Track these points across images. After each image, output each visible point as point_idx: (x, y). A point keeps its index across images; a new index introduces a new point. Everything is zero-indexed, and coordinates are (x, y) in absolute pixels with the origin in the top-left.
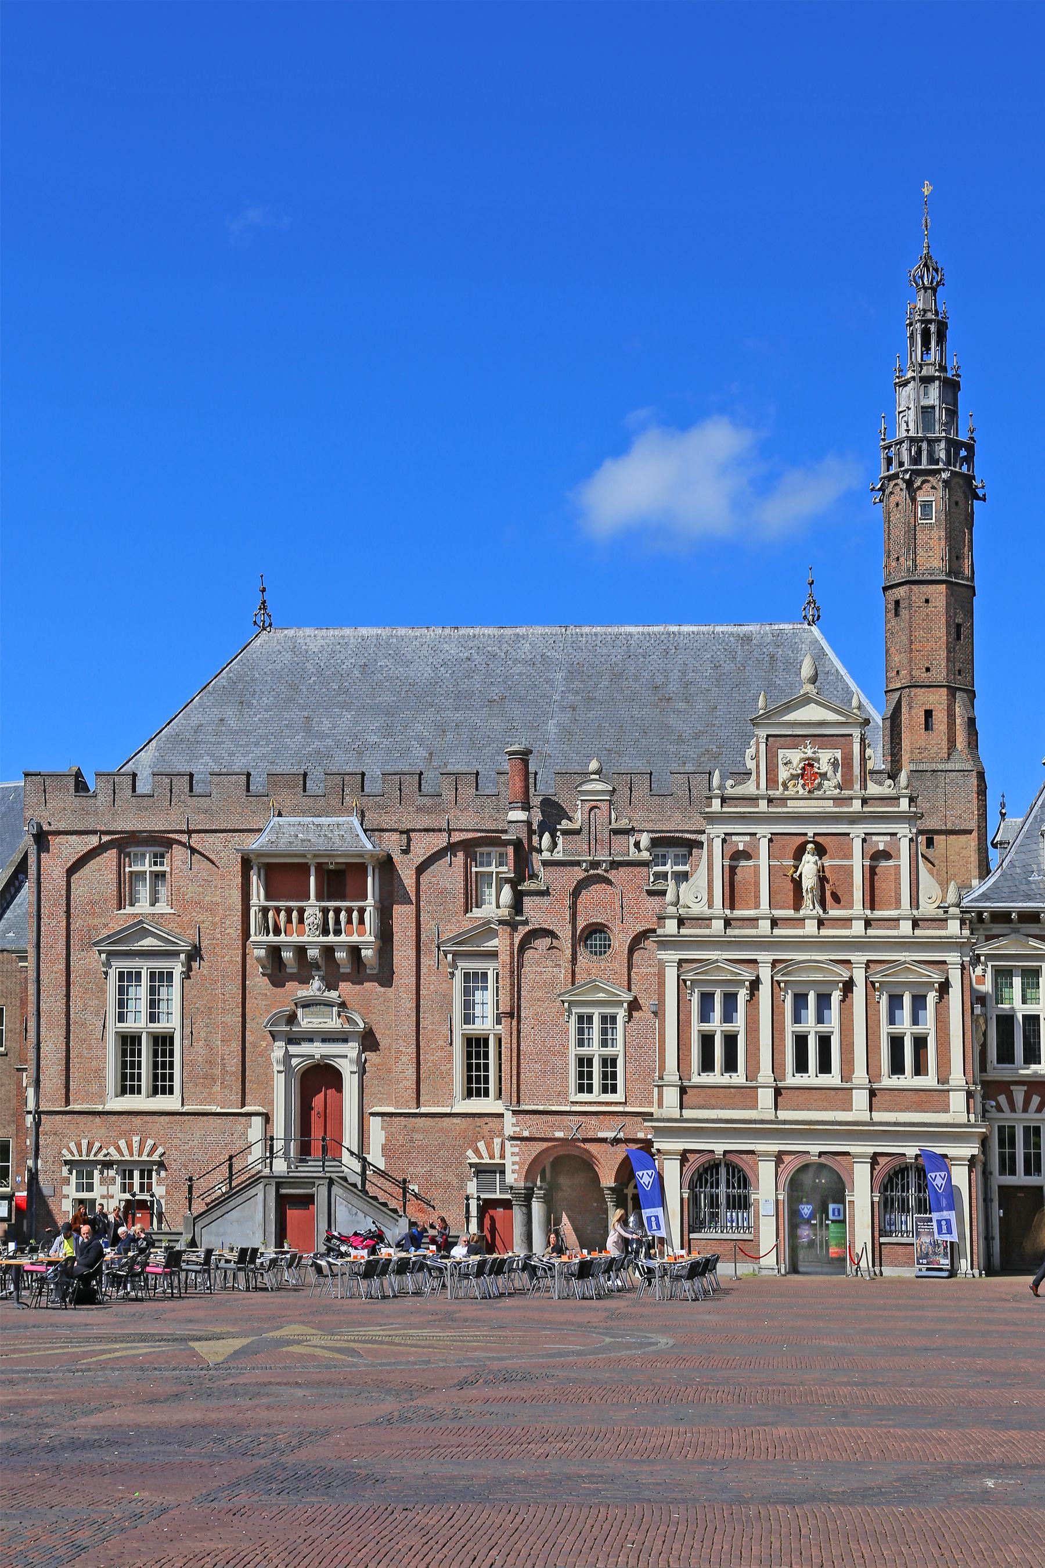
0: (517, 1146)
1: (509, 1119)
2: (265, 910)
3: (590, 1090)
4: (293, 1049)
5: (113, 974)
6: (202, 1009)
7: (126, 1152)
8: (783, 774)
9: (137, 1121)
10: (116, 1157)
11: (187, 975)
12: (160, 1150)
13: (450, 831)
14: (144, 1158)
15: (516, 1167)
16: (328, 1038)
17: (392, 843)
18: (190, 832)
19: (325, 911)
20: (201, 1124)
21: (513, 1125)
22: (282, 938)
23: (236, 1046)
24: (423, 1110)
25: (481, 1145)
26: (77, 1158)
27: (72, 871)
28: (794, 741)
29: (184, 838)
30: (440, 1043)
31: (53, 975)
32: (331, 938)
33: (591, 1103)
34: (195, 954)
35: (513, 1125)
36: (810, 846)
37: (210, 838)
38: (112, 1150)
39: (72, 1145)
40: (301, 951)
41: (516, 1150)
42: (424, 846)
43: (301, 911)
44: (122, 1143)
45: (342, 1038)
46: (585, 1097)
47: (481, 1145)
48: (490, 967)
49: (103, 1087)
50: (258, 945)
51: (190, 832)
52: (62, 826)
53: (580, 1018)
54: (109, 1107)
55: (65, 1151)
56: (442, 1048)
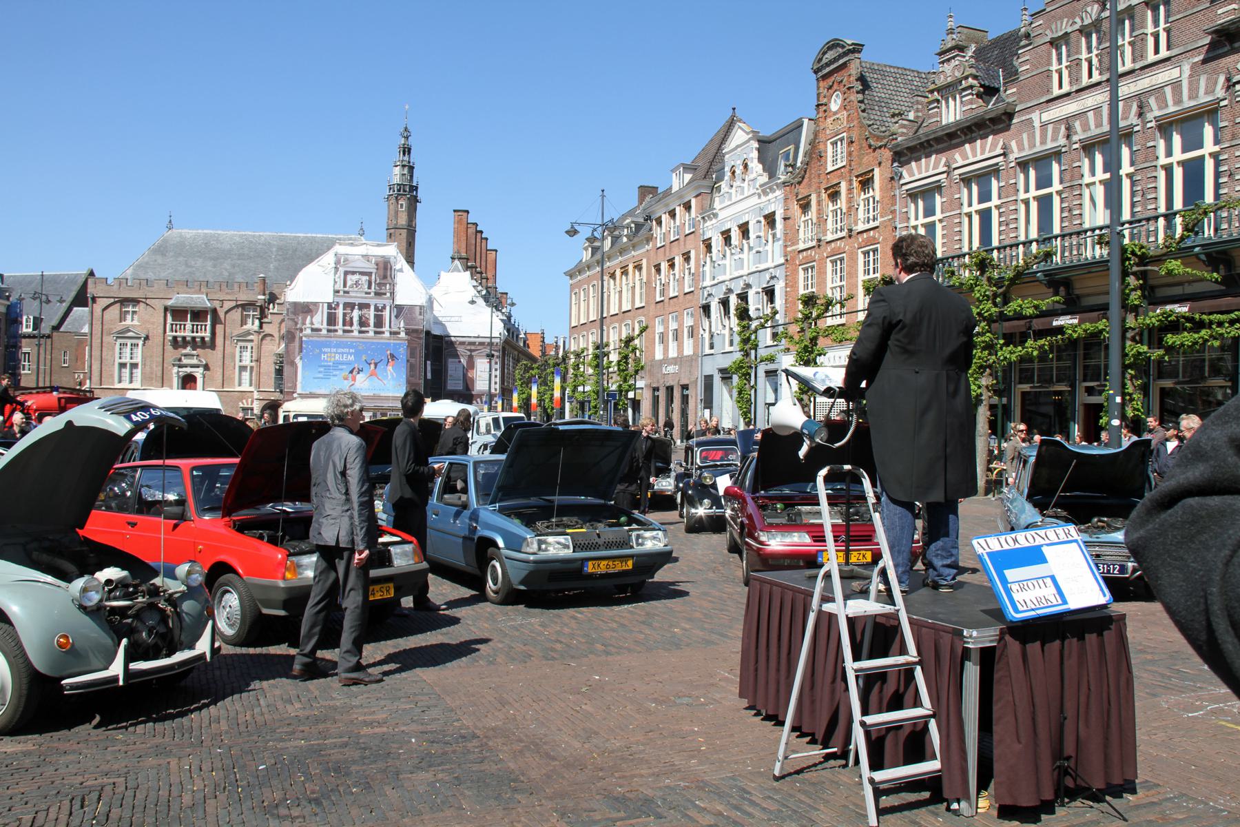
2: (172, 325)
4: (180, 370)
5: (118, 344)
8: (349, 283)
11: (144, 345)
13: (237, 301)
16: (193, 366)
17: (217, 304)
18: (146, 298)
19: (193, 325)
22: (178, 334)
23: (160, 368)
24: (225, 390)
25: (244, 401)
27: (104, 310)
28: (353, 273)
29: (144, 300)
32: (195, 334)
34: (147, 338)
36: (356, 307)
37: (154, 300)
40: (184, 338)
42: (228, 305)
43: (185, 325)
45: (197, 366)
47: (244, 401)
48: (249, 345)
49: (113, 380)
50: (169, 336)
51: (146, 298)
52: (101, 295)
54: (115, 387)
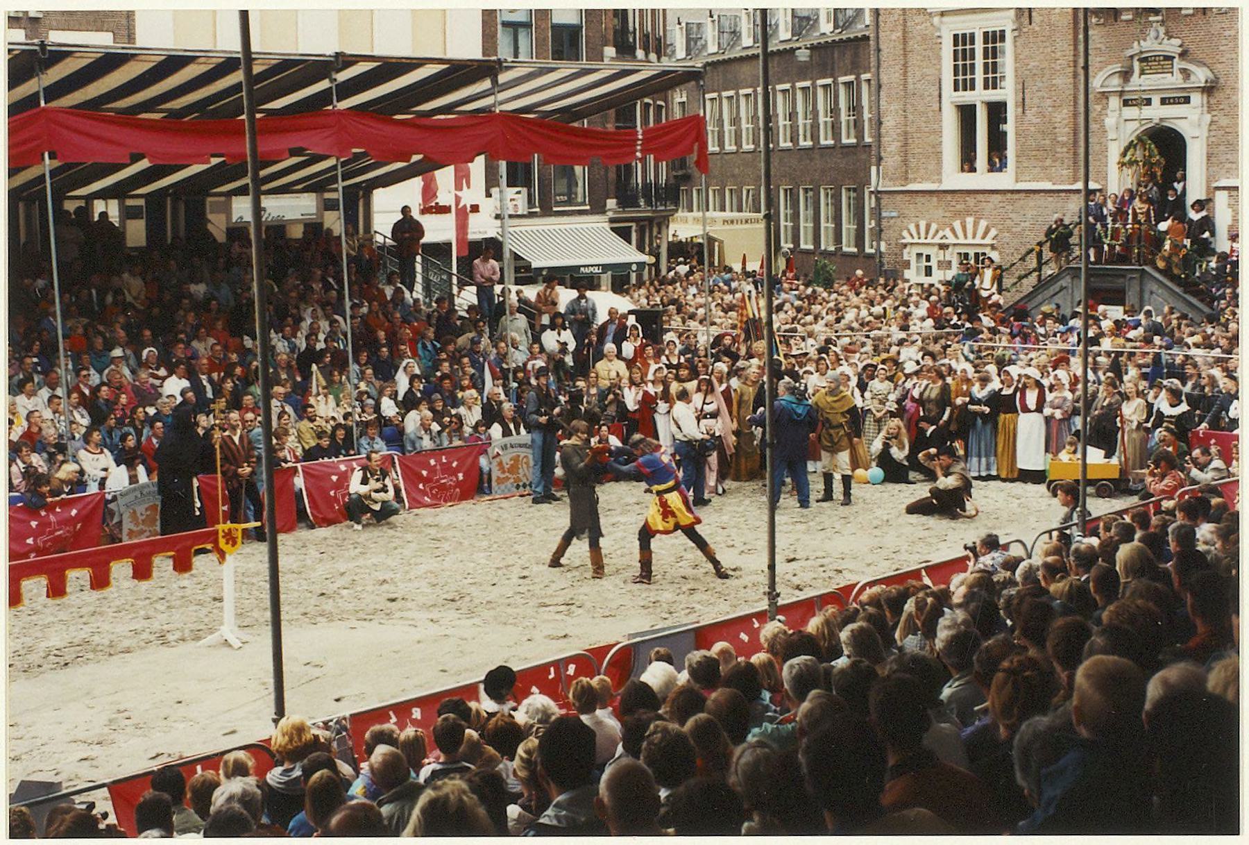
6: (1034, 71)
9: (971, 201)
10: (951, 240)
12: (993, 232)
14: (978, 241)
20: (1032, 204)
26: (916, 240)
31: (892, 44)
38: (948, 232)
39: (912, 227)
44: (957, 225)
55: (905, 233)
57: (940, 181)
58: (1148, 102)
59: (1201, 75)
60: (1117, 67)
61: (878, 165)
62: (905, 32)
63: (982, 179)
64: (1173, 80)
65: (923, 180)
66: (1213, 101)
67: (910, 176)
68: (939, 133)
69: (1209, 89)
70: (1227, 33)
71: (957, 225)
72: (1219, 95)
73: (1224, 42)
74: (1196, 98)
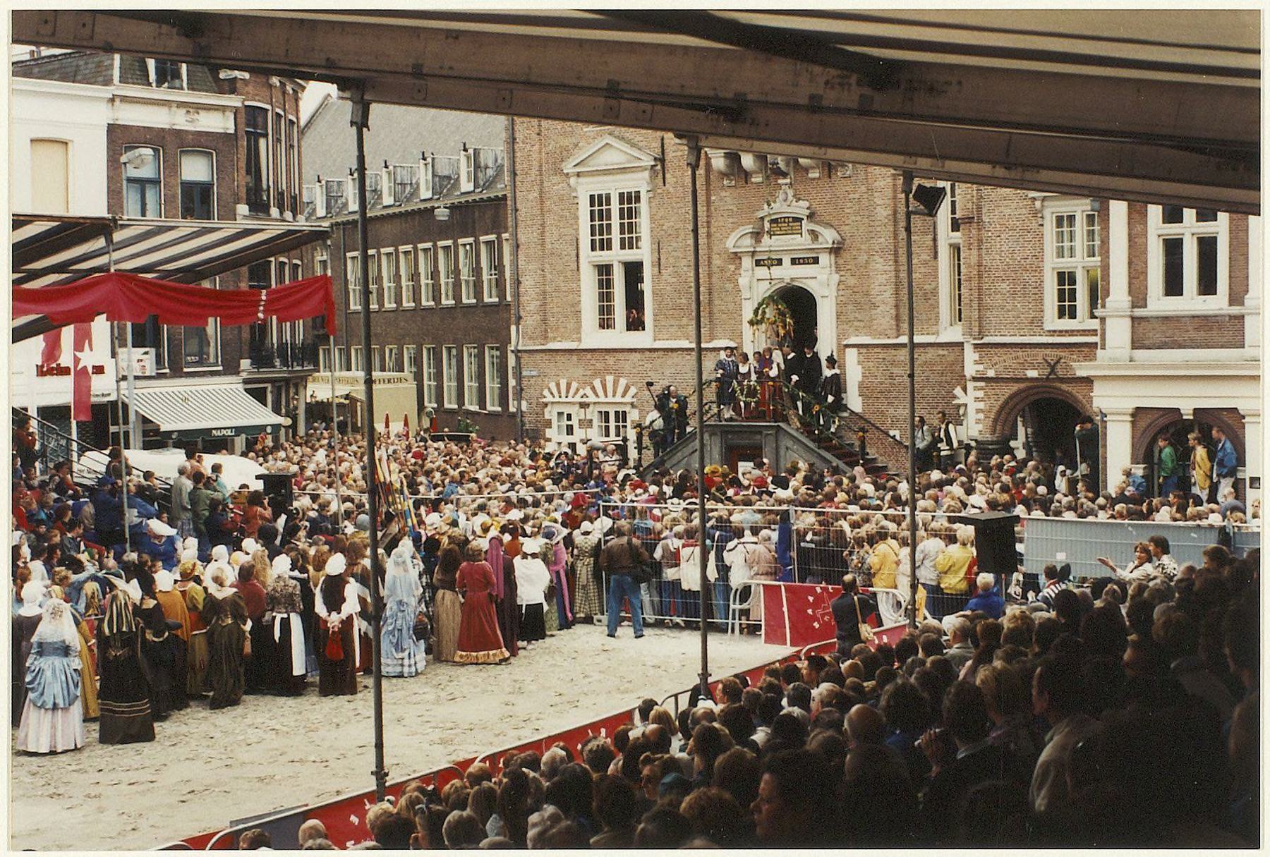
0: (981, 389)
1: (970, 355)
3: (1073, 315)
4: (762, 272)
6: (670, 232)
7: (600, 392)
9: (611, 359)
10: (592, 398)
12: (633, 390)
14: (618, 399)
15: (981, 416)
20: (670, 362)
21: (976, 362)
26: (557, 399)
30: (925, 257)
31: (529, 204)
33: (1071, 333)
35: (976, 362)
38: (588, 391)
39: (553, 386)
41: (980, 394)
44: (597, 383)
46: (1067, 324)
53: (1060, 221)
55: (546, 392)
56: (925, 263)
57: (580, 340)
58: (780, 262)
59: (829, 236)
60: (749, 229)
61: (518, 324)
62: (541, 192)
63: (619, 337)
64: (801, 241)
65: (563, 338)
66: (841, 261)
67: (550, 335)
68: (578, 292)
69: (836, 250)
70: (851, 196)
71: (597, 383)
72: (846, 256)
73: (849, 205)
74: (825, 259)
